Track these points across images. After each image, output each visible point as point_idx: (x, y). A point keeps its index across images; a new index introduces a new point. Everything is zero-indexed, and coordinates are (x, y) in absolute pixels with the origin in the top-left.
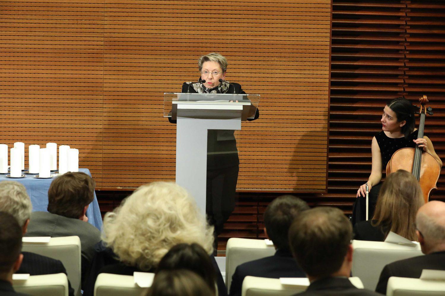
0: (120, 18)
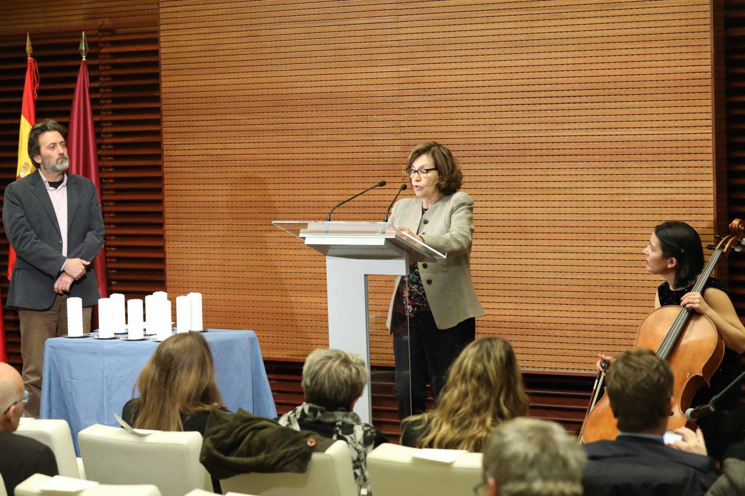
0: (420, 111)
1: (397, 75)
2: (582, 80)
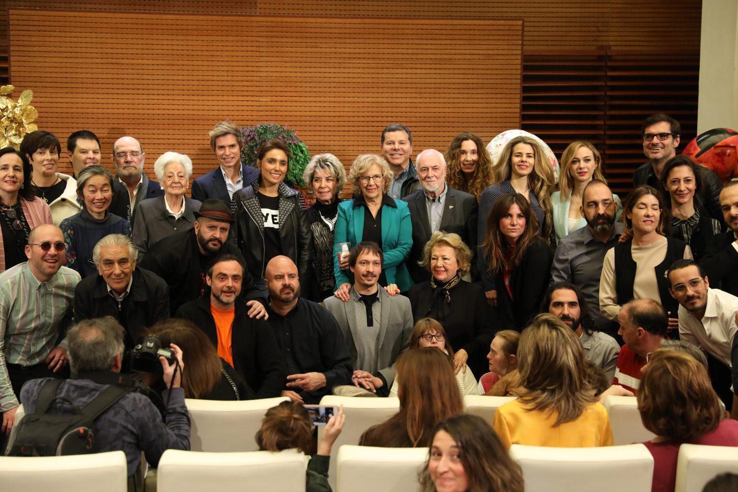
1: (258, 104)
2: (417, 115)
